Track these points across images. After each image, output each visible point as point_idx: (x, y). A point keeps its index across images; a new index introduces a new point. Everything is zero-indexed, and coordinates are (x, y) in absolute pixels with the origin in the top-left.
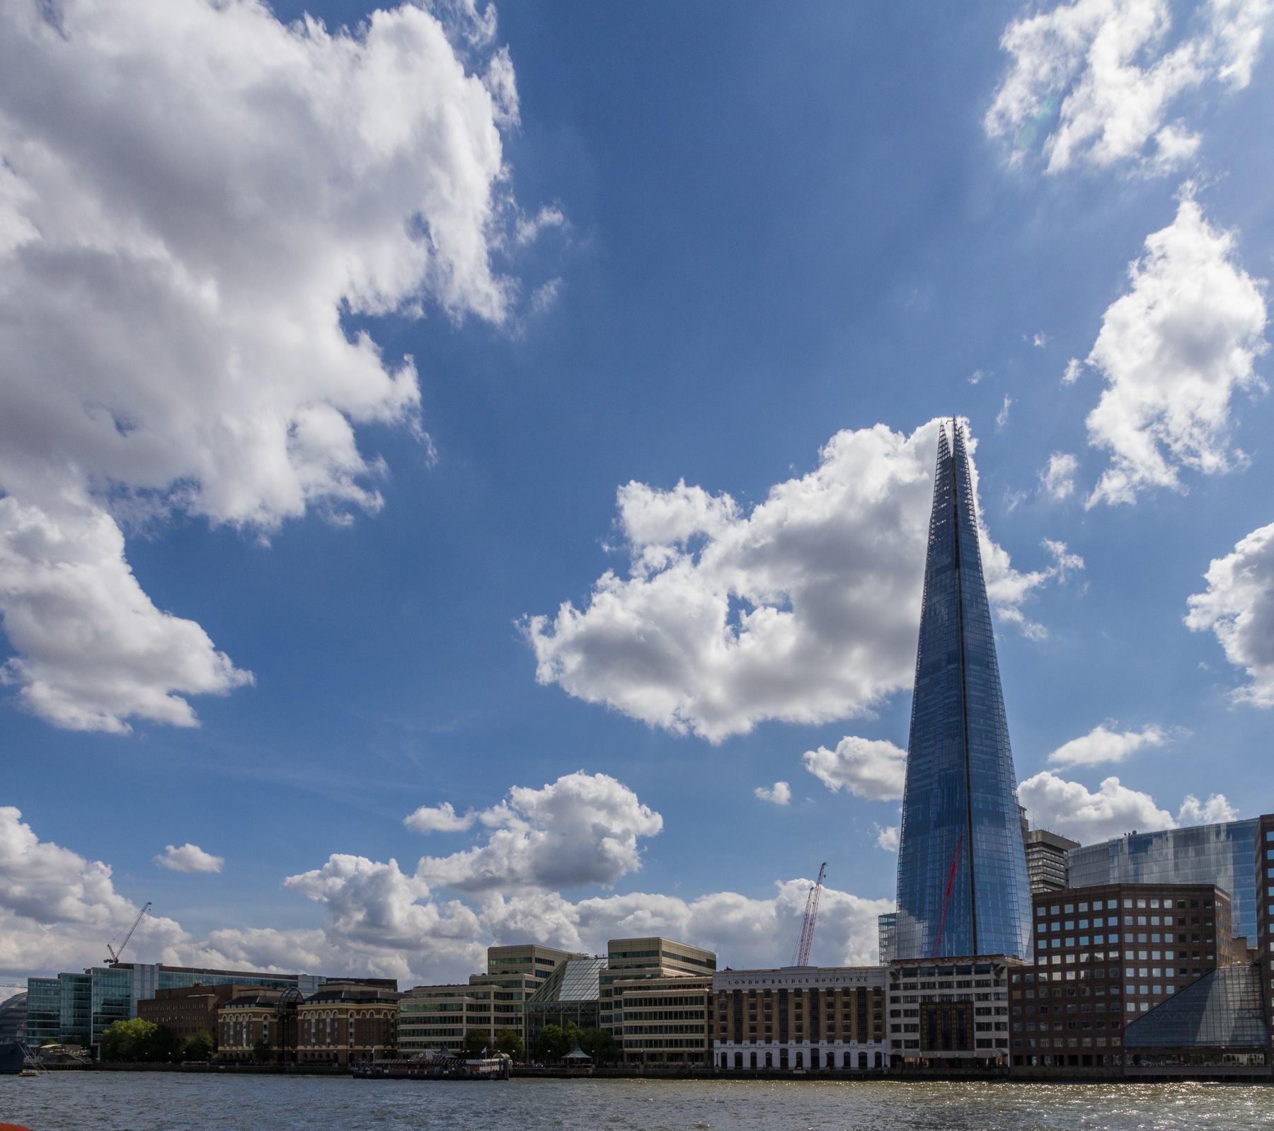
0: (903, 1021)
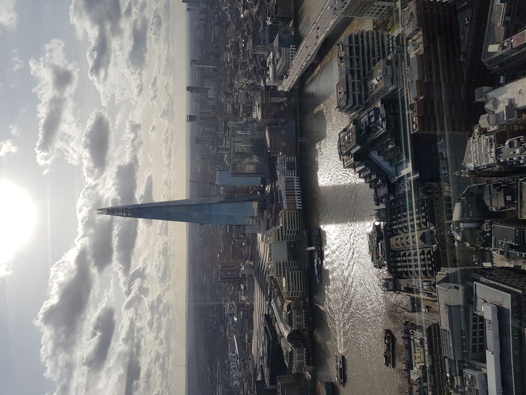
0: (291, 174)
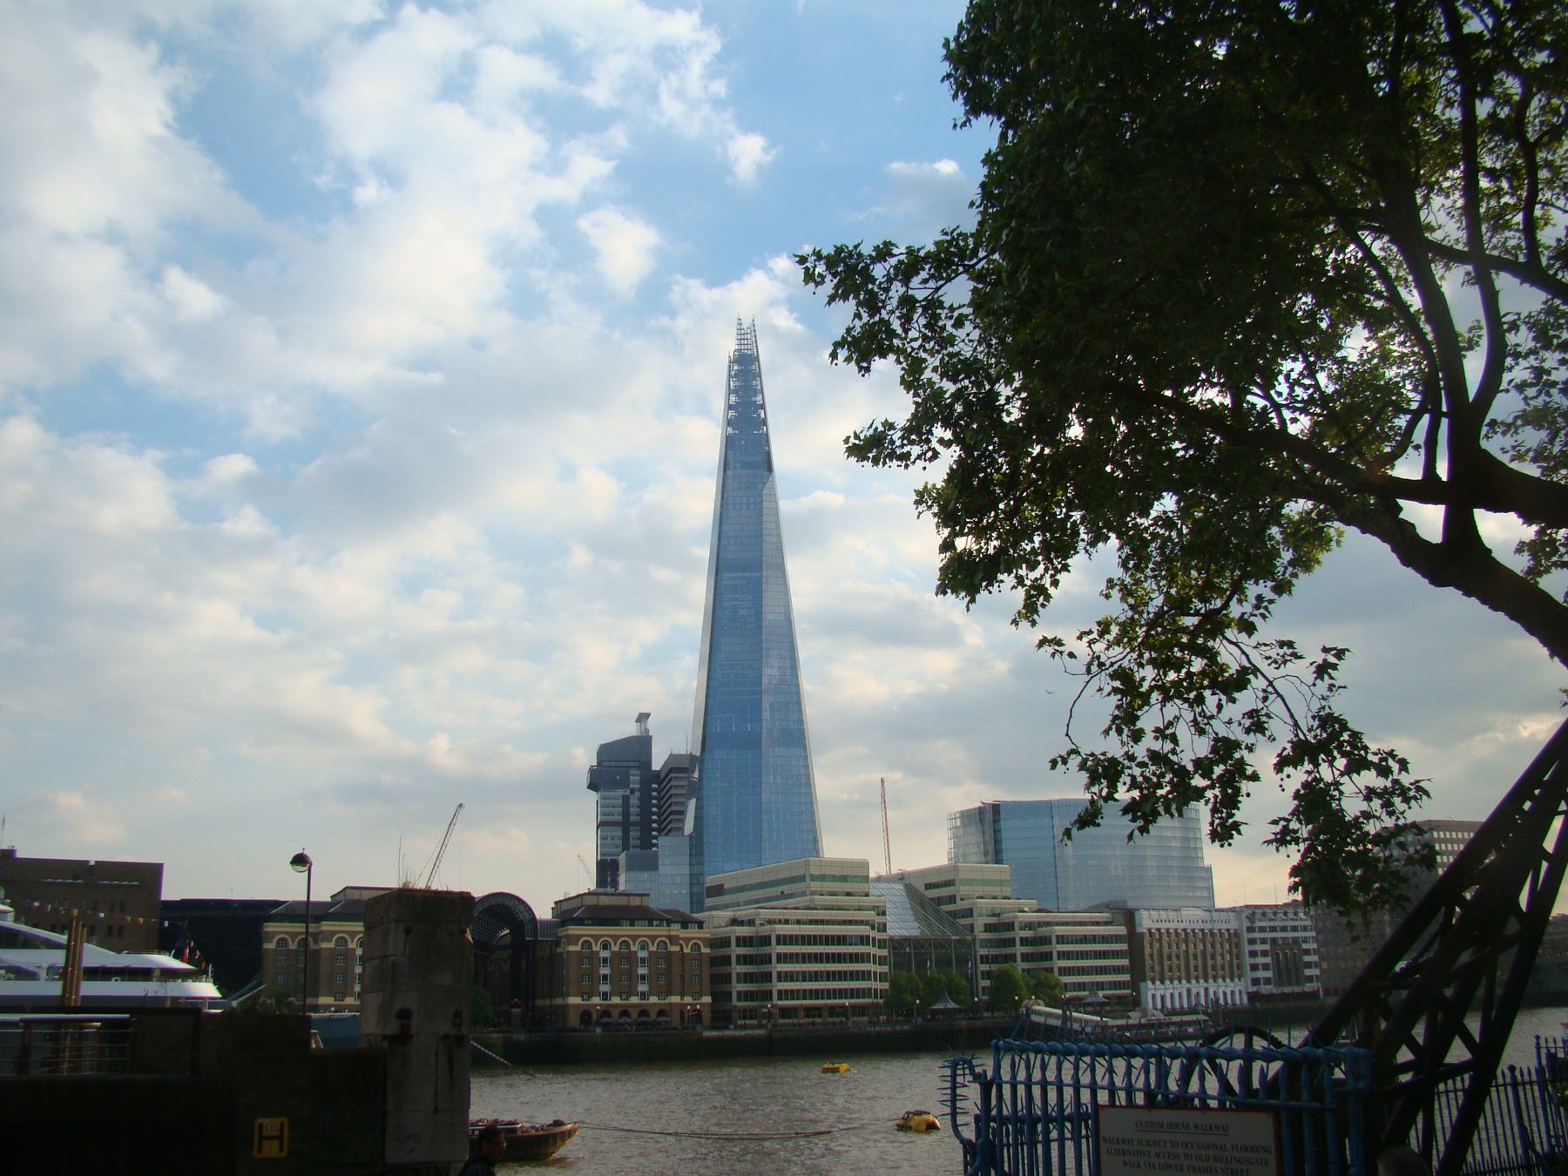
0: (1260, 960)
